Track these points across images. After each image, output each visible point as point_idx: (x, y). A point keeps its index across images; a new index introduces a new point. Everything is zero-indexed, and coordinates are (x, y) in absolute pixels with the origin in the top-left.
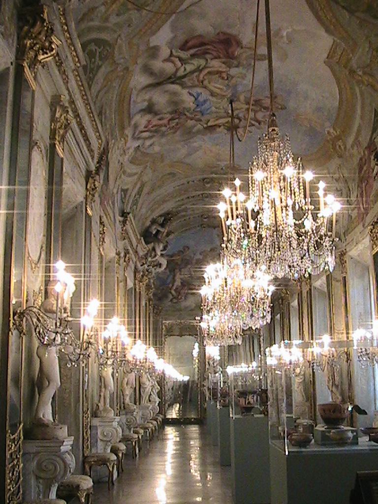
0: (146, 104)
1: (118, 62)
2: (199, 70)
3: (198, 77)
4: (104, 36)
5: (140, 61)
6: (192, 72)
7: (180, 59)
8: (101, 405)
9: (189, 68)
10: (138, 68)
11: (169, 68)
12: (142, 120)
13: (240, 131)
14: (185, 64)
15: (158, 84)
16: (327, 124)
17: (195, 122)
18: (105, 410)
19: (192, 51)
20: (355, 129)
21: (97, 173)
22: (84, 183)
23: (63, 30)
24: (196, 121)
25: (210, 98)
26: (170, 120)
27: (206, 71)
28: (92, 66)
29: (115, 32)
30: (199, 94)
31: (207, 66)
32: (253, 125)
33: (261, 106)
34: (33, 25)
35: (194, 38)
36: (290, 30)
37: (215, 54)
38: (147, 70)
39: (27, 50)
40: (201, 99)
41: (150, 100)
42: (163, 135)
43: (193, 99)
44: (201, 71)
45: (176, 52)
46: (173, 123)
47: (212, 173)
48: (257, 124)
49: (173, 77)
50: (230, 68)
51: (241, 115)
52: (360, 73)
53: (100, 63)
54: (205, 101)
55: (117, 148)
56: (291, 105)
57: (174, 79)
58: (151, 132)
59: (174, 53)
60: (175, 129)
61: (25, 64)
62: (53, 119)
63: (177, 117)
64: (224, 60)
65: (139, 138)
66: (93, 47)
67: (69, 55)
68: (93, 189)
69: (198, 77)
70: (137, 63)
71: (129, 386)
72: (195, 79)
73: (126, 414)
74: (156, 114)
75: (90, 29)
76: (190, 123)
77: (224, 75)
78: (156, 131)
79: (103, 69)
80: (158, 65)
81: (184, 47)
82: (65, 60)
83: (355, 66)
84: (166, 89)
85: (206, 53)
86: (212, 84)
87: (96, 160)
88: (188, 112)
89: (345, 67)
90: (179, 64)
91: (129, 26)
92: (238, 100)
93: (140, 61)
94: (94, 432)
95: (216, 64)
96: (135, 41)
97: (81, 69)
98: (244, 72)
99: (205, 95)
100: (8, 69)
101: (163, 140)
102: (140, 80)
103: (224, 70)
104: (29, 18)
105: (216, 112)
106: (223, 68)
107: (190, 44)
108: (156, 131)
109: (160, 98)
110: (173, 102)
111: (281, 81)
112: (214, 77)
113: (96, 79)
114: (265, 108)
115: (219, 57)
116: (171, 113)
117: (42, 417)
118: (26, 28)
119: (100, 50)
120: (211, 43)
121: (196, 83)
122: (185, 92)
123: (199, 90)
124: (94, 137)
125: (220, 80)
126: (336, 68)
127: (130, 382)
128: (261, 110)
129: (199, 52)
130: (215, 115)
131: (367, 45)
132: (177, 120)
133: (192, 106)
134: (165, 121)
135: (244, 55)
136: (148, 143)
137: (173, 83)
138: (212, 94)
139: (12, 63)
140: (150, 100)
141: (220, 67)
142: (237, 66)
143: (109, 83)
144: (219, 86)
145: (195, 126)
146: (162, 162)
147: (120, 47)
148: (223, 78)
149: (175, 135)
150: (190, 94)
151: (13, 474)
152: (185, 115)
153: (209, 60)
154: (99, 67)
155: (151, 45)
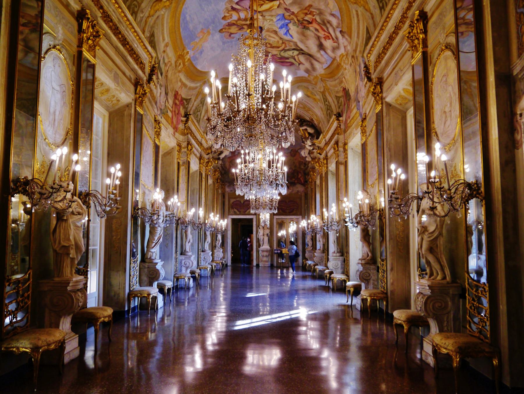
3: (286, 47)
6: (289, 50)
7: (295, 60)
9: (290, 53)
11: (302, 58)
12: (328, 44)
15: (310, 55)
17: (290, 8)
24: (289, 10)
25: (277, 30)
26: (311, 23)
27: (280, 49)
32: (237, 3)
33: (238, 25)
38: (314, 69)
40: (284, 30)
41: (319, 51)
42: (321, 13)
43: (290, 31)
44: (283, 49)
46: (308, 18)
48: (235, 6)
54: (281, 28)
56: (217, 36)
58: (327, 29)
59: (298, 65)
63: (304, 22)
65: (337, 38)
69: (286, 47)
72: (287, 45)
74: (319, 38)
76: (295, 9)
77: (269, 46)
78: (325, 24)
80: (307, 65)
81: (292, 64)
85: (280, 58)
86: (276, 40)
88: (295, 22)
90: (296, 57)
101: (323, 7)
103: (269, 49)
105: (272, 16)
108: (325, 24)
109: (312, 46)
110: (305, 36)
111: (232, 47)
114: (234, 24)
116: (308, 28)
121: (287, 43)
122: (295, 40)
125: (271, 42)
128: (236, 21)
130: (273, 13)
132: (306, 18)
133: (291, 26)
134: (315, 25)
136: (334, 21)
137: (302, 50)
138: (276, 32)
140: (319, 51)
148: (269, 44)
149: (311, 3)
150: (291, 36)
152: (298, 20)
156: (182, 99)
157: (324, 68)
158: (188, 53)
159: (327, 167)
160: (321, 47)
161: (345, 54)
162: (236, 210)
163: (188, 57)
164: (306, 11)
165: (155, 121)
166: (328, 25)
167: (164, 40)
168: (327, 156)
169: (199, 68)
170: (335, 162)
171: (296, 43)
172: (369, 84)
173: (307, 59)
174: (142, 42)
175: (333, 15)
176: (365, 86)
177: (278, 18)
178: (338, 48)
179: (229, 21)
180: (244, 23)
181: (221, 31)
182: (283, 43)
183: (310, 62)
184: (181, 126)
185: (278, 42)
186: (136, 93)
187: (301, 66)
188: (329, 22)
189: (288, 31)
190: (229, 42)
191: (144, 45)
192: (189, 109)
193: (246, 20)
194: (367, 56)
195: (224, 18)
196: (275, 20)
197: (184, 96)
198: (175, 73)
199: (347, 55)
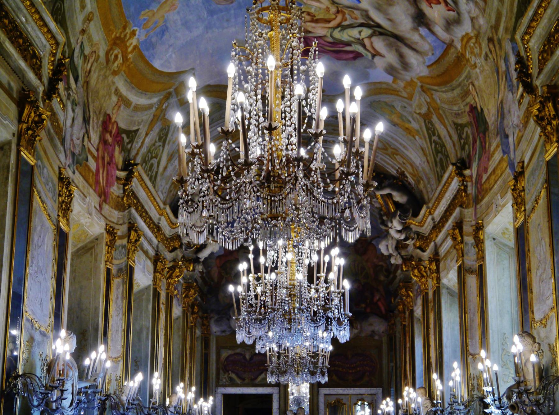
2: (342, 27)
3: (344, 19)
6: (351, 26)
7: (364, 46)
9: (354, 33)
11: (379, 44)
14: (359, 39)
27: (332, 24)
31: (330, 30)
35: (346, 60)
41: (415, 29)
44: (339, 25)
45: (367, 55)
49: (377, 33)
57: (378, 30)
64: (310, 35)
72: (347, 16)
77: (308, 18)
80: (391, 58)
81: (357, 56)
86: (324, 7)
90: (367, 42)
103: (308, 24)
106: (310, 26)
107: (351, 56)
111: (228, 20)
112: (321, 16)
125: (312, 11)
129: (341, 46)
137: (379, 26)
140: (415, 29)
141: (314, 28)
148: (309, 14)
153: (329, 35)
156: (120, 132)
157: (428, 63)
158: (133, 33)
159: (438, 279)
160: (420, 19)
161: (472, 35)
162: (233, 376)
163: (134, 41)
165: (61, 179)
167: (83, 7)
168: (436, 253)
169: (157, 64)
170: (456, 268)
172: (527, 98)
173: (390, 46)
174: (37, 12)
176: (520, 103)
178: (458, 21)
182: (338, 12)
184: (116, 190)
185: (328, 9)
186: (20, 121)
187: (377, 59)
190: (221, 11)
191: (41, 19)
192: (133, 153)
194: (523, 39)
197: (122, 125)
198: (105, 77)
199: (477, 36)
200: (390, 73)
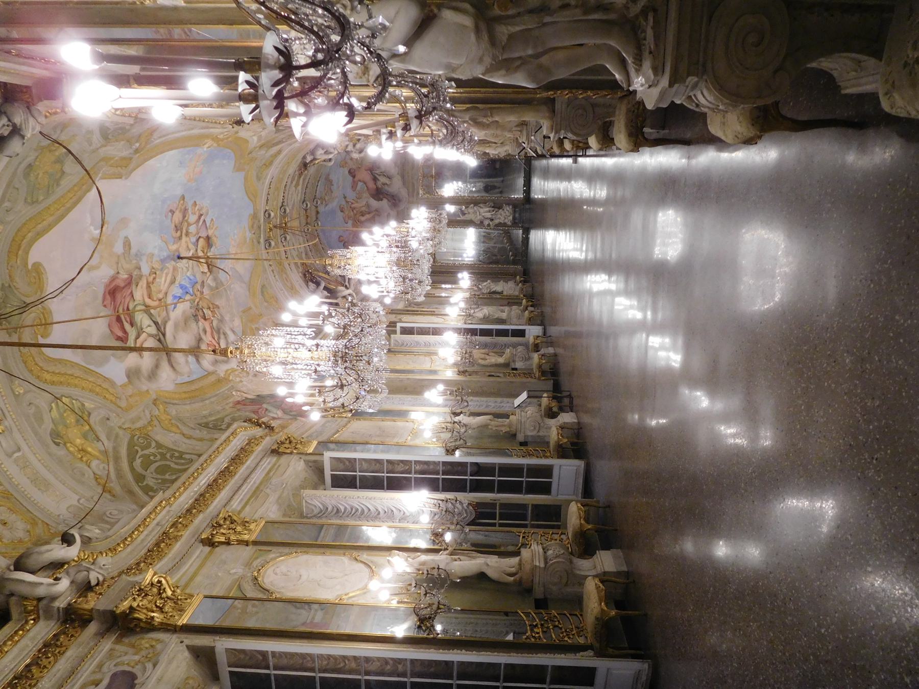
0: (191, 359)
1: (149, 417)
3: (155, 308)
4: (123, 452)
5: (144, 388)
6: (151, 316)
7: (138, 337)
8: (504, 429)
10: (153, 386)
13: (210, 233)
16: (199, 151)
18: (510, 426)
19: (127, 326)
20: (202, 131)
21: (272, 429)
22: (284, 459)
23: (132, 542)
25: (177, 282)
26: (205, 319)
27: (149, 302)
28: (159, 457)
29: (117, 436)
30: (175, 297)
34: (139, 620)
36: (92, 228)
37: (128, 299)
38: (153, 374)
39: (165, 621)
42: (221, 321)
47: (259, 242)
48: (202, 218)
50: (142, 276)
51: (194, 239)
52: (137, 145)
53: (153, 444)
54: (182, 287)
55: (240, 384)
56: (179, 192)
58: (219, 338)
60: (213, 307)
61: (180, 623)
62: (228, 543)
66: (138, 462)
67: (155, 522)
68: (290, 442)
69: (155, 308)
70: (147, 391)
71: (487, 357)
73: (514, 361)
74: (200, 340)
75: (120, 475)
77: (151, 279)
78: (218, 332)
79: (158, 438)
82: (162, 526)
83: (131, 151)
84: (172, 338)
87: (258, 431)
89: (131, 159)
90: (144, 336)
91: (108, 419)
92: (177, 250)
93: (144, 386)
94: (530, 439)
95: (139, 293)
96: (123, 404)
97: (169, 493)
98: (144, 259)
99: (176, 291)
100: (187, 646)
101: (227, 318)
102: (166, 380)
104: (132, 626)
106: (143, 283)
107: (120, 334)
108: (218, 332)
113: (171, 446)
114: (184, 217)
115: (132, 292)
116: (197, 321)
117: (512, 578)
118: (142, 624)
119: (139, 450)
120: (116, 309)
123: (170, 300)
124: (235, 441)
125: (157, 280)
126: (131, 166)
127: (483, 356)
131: (104, 149)
134: (207, 325)
135: (127, 266)
136: (232, 337)
137: (164, 335)
138: (173, 282)
139: (182, 642)
142: (140, 269)
143: (173, 421)
144: (163, 279)
145: (209, 286)
146: (250, 308)
147: (133, 422)
148: (154, 278)
151: (561, 629)
154: (159, 445)
155: (126, 380)
164: (211, 306)
166: (222, 336)
171: (169, 319)
175: (233, 332)
177: (192, 278)
179: (190, 211)
180: (184, 231)
181: (183, 198)
182: (160, 300)
183: (157, 360)
185: (160, 291)
188: (224, 334)
189: (180, 298)
193: (187, 234)
195: (195, 204)
196: (188, 274)
200: (128, 377)
